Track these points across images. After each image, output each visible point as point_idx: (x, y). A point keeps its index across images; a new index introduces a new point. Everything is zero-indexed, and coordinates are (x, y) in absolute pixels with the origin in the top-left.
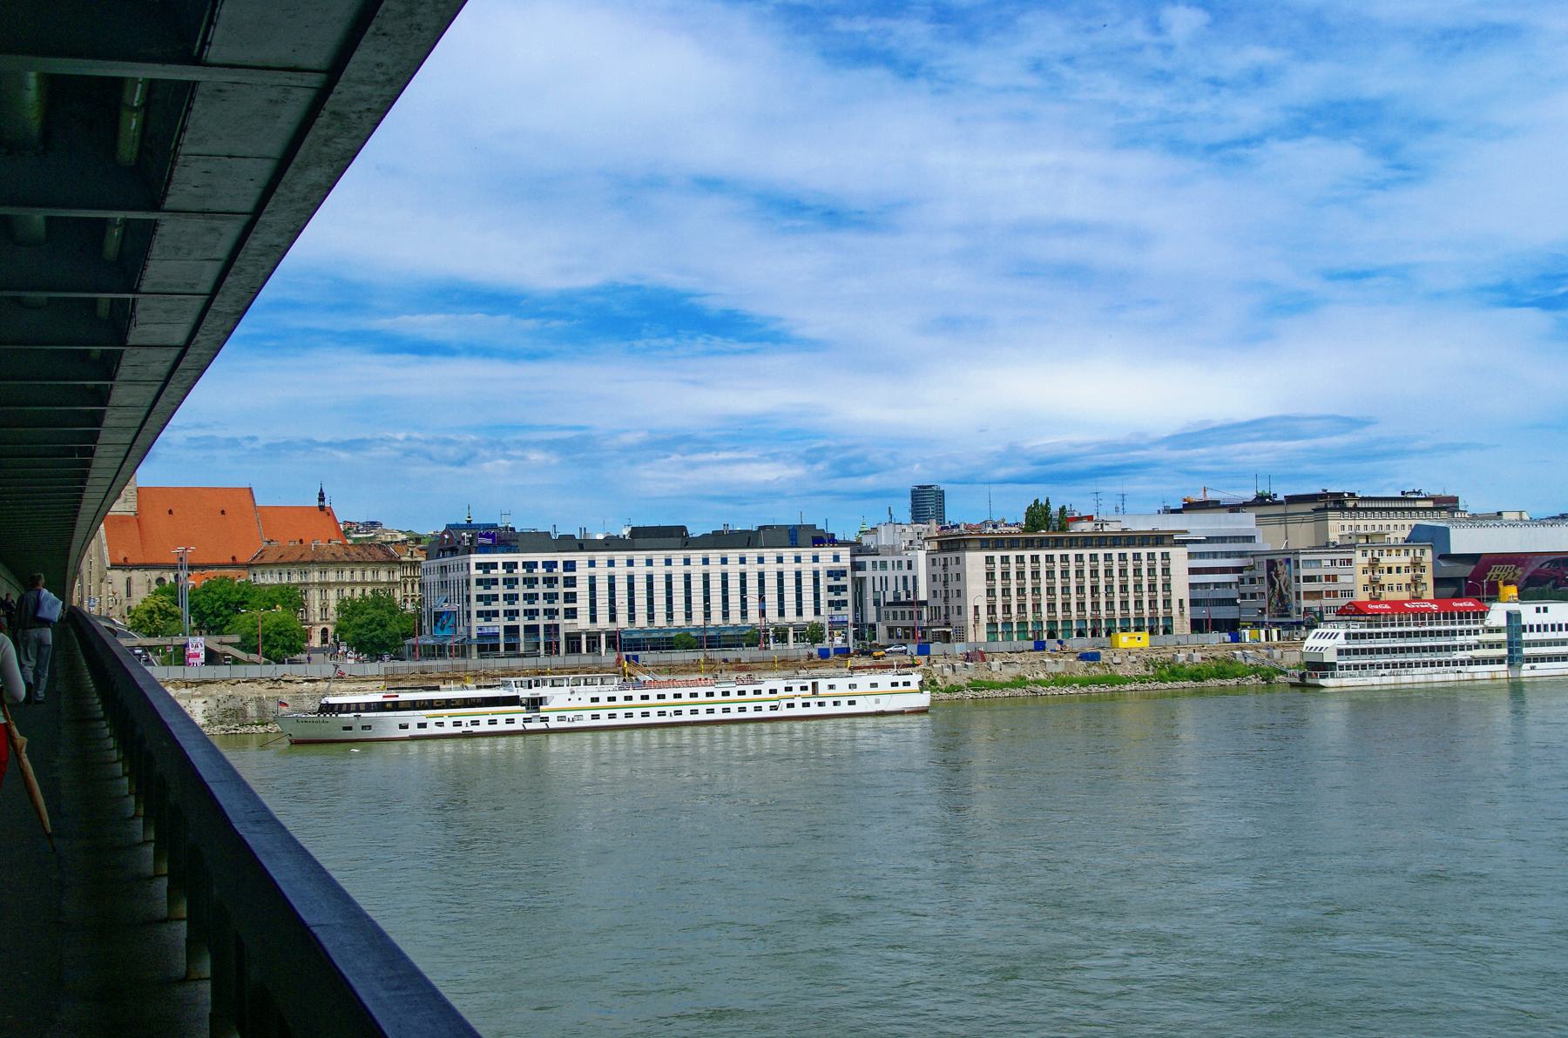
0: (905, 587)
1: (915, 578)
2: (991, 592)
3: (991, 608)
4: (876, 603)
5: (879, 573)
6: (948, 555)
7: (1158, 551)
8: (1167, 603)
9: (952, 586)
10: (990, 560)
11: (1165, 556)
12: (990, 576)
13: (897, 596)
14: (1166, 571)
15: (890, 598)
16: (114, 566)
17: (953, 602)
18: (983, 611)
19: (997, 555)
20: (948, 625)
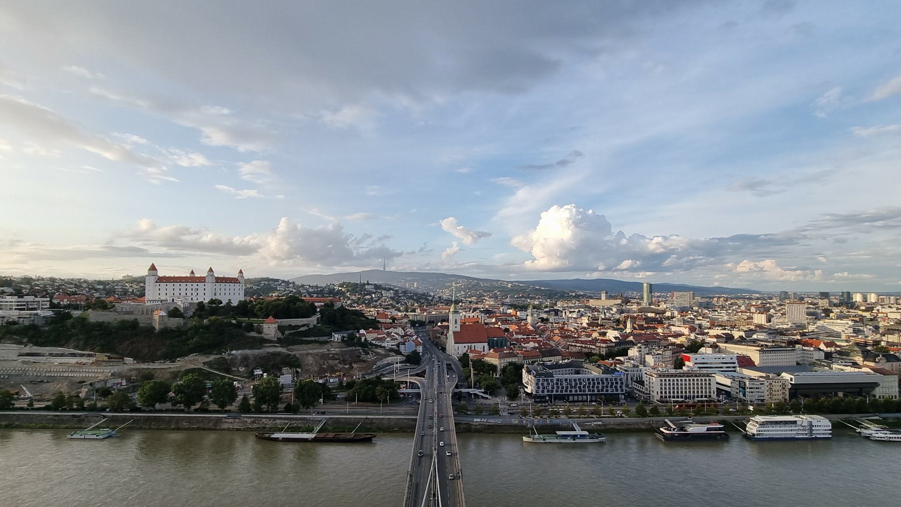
0: (639, 376)
1: (642, 374)
2: (661, 388)
3: (661, 393)
4: (632, 379)
5: (632, 373)
6: (651, 377)
7: (707, 378)
8: (710, 392)
9: (651, 384)
10: (661, 380)
11: (710, 380)
12: (661, 385)
13: (637, 379)
14: (709, 384)
15: (635, 380)
16: (455, 343)
17: (651, 389)
18: (659, 393)
19: (663, 379)
20: (650, 394)
